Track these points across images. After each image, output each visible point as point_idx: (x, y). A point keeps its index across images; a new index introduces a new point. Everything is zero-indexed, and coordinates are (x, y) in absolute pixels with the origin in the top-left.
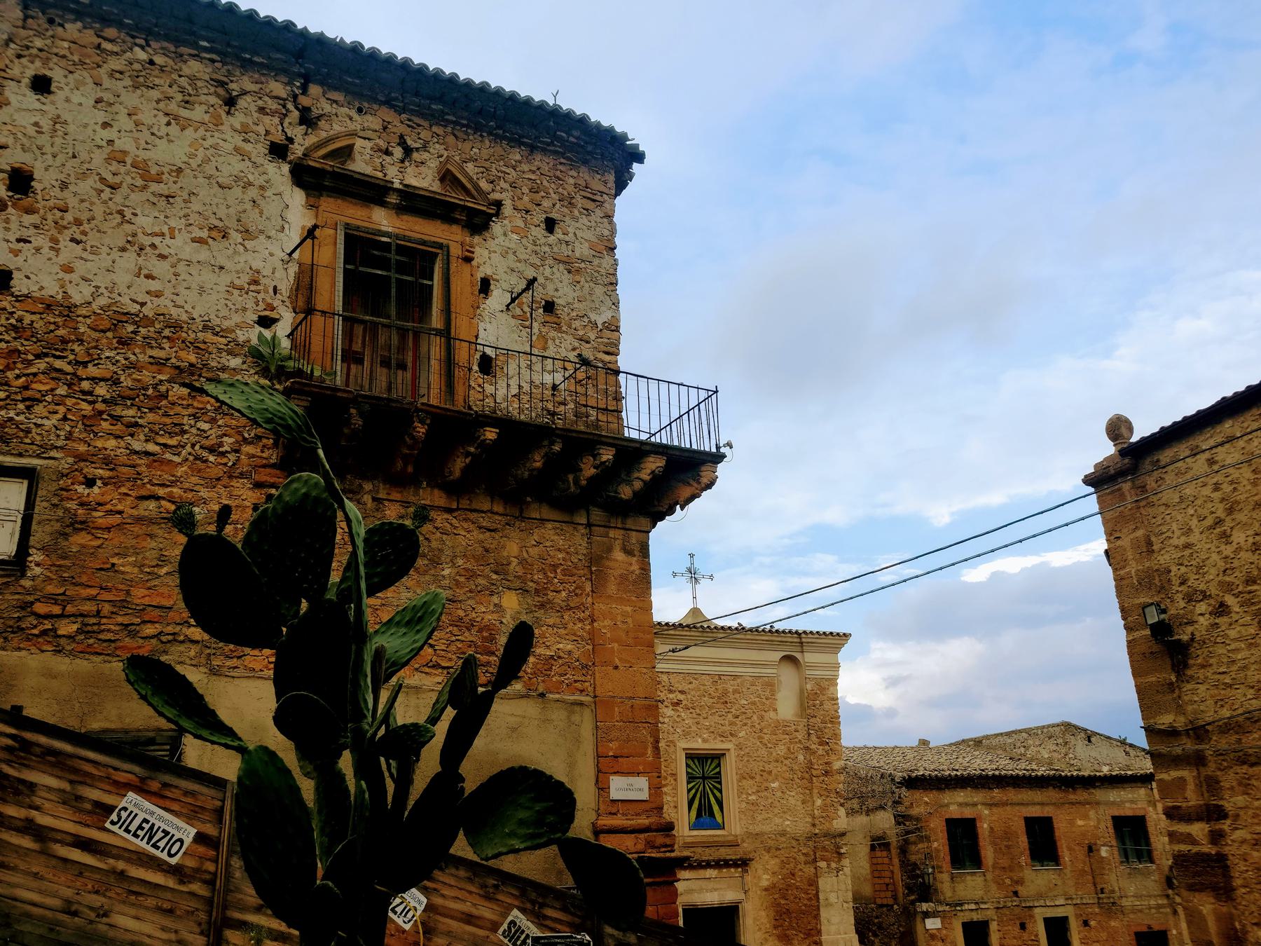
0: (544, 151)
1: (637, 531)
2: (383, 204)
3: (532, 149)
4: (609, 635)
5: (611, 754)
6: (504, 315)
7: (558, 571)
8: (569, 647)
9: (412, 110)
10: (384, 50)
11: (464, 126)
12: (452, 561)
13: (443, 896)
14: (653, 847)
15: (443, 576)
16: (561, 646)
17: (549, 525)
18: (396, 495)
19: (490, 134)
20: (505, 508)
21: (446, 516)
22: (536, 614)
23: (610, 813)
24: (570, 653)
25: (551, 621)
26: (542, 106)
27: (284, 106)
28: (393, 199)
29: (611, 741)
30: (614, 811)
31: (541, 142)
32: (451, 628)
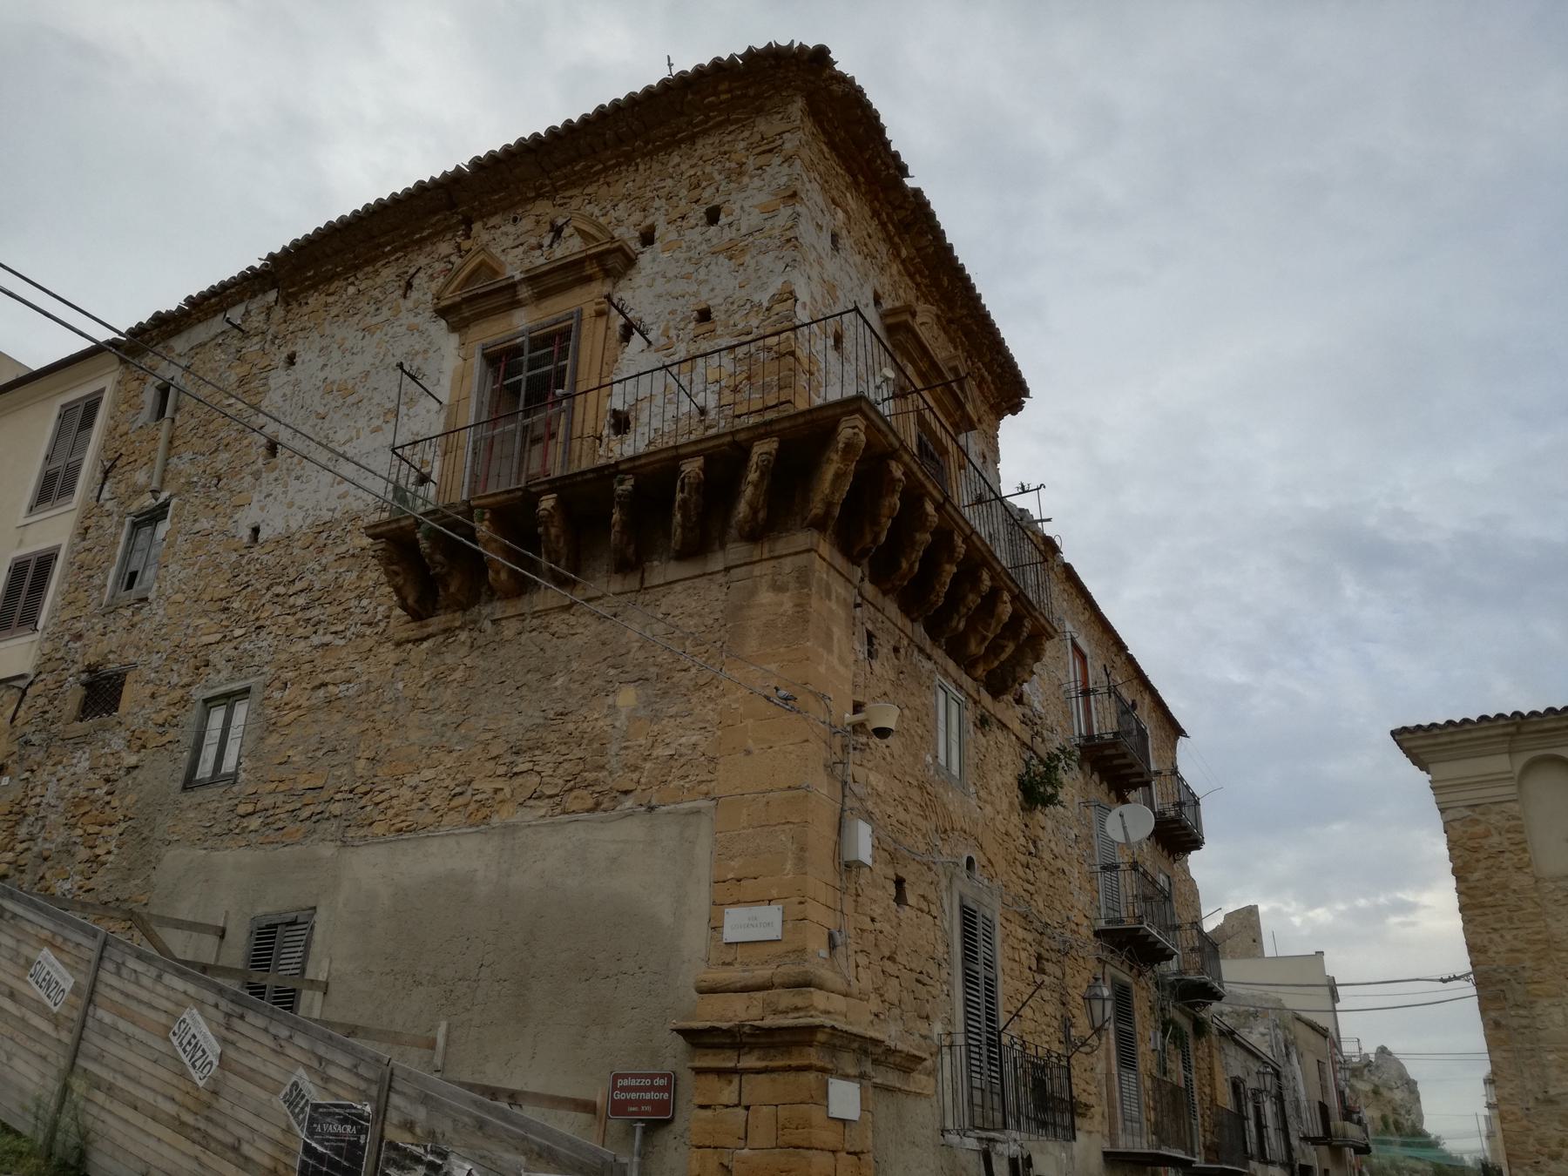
0: (706, 132)
1: (790, 555)
2: (516, 304)
3: (692, 139)
4: (741, 710)
5: (730, 876)
6: (646, 354)
7: (687, 643)
8: (694, 739)
9: (562, 186)
10: (497, 147)
11: (615, 166)
12: (565, 667)
13: (238, 1048)
14: (775, 1012)
15: (556, 688)
16: (683, 740)
17: (678, 587)
18: (511, 611)
19: (644, 156)
20: (623, 585)
21: (565, 616)
22: (656, 706)
23: (724, 964)
24: (695, 745)
25: (672, 711)
26: (665, 85)
27: (450, 262)
28: (524, 292)
29: (731, 858)
30: (728, 960)
31: (696, 126)
32: (558, 748)
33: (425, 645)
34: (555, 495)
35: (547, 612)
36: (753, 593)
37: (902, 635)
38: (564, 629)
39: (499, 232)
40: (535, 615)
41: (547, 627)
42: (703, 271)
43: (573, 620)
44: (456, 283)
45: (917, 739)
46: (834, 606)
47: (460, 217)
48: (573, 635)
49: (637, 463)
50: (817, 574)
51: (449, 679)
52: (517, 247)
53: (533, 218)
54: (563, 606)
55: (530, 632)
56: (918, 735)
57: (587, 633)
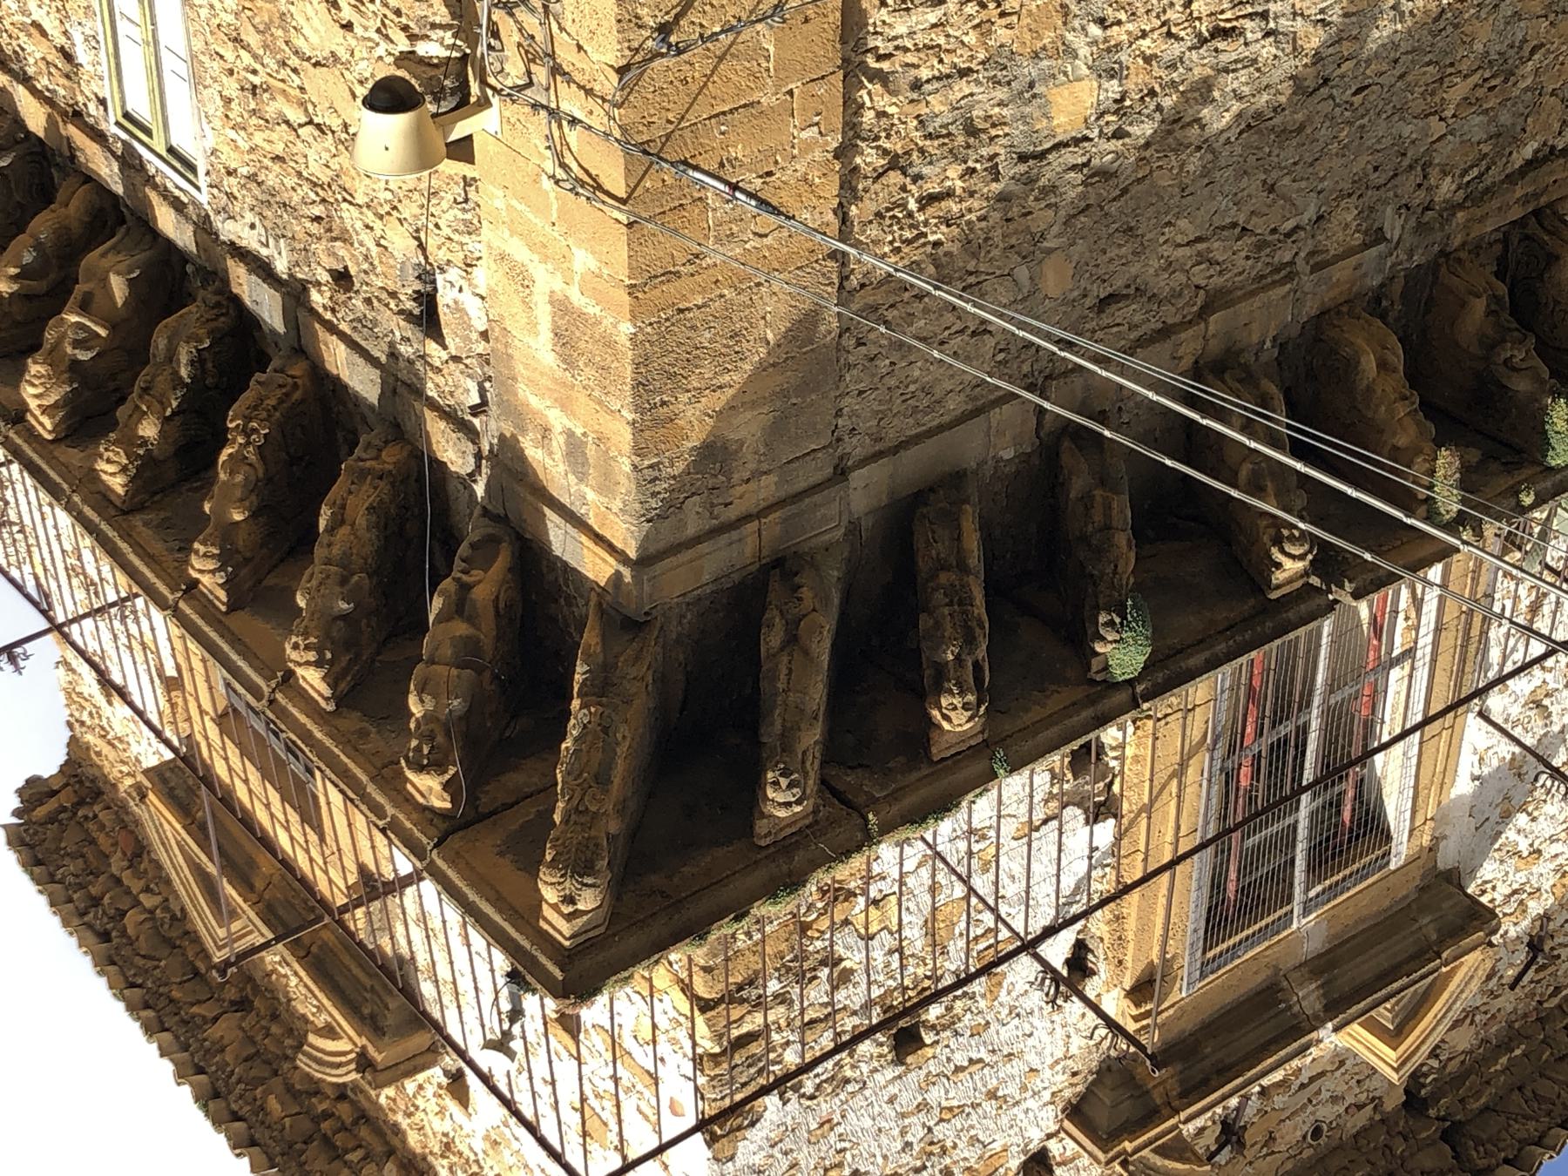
2: (1323, 965)
28: (1308, 996)
33: (1528, 152)
34: (1274, 595)
35: (1261, 283)
36: (776, 431)
37: (328, 316)
38: (1217, 249)
39: (1350, 1100)
40: (1288, 272)
41: (1260, 246)
42: (916, 1134)
43: (1199, 275)
44: (1452, 986)
45: (252, 39)
46: (557, 420)
47: (1432, 1112)
48: (1199, 240)
49: (1087, 713)
50: (617, 505)
51: (1476, 78)
52: (1312, 1079)
53: (1280, 1146)
54: (1230, 304)
55: (1297, 228)
56: (246, 48)
57: (1166, 250)
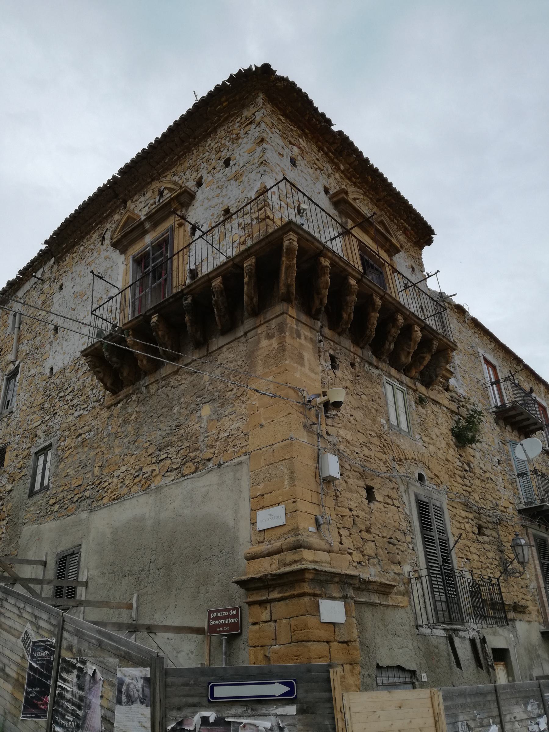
3: (215, 130)
4: (257, 405)
5: (259, 494)
12: (178, 402)
13: (5, 617)
14: (285, 565)
15: (174, 413)
17: (224, 349)
19: (195, 145)
22: (219, 412)
23: (259, 542)
25: (226, 413)
28: (147, 226)
30: (261, 540)
33: (119, 405)
34: (157, 314)
35: (168, 376)
36: (259, 342)
37: (355, 356)
38: (176, 383)
39: (138, 202)
40: (163, 379)
41: (169, 384)
42: (224, 190)
43: (179, 378)
44: (118, 229)
45: (373, 411)
46: (303, 341)
47: (121, 200)
48: (180, 385)
49: (192, 288)
50: (289, 325)
51: (130, 419)
52: (146, 206)
53: (151, 191)
54: (174, 372)
55: (162, 388)
56: (374, 409)
57: (186, 382)
